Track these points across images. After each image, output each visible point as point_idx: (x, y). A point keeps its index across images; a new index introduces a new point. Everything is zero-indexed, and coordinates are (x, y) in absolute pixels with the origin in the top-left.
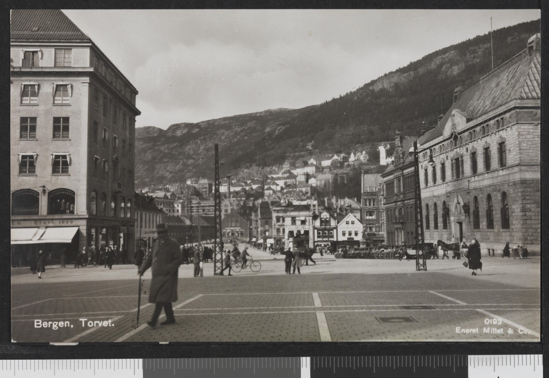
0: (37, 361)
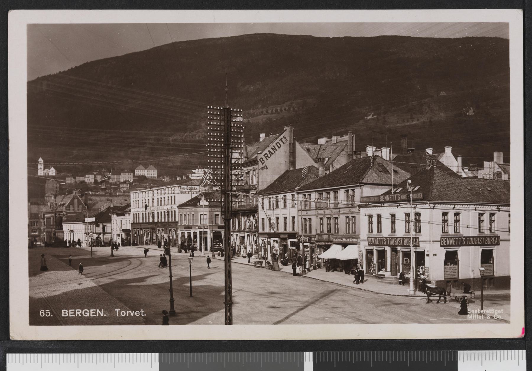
0: (62, 354)
